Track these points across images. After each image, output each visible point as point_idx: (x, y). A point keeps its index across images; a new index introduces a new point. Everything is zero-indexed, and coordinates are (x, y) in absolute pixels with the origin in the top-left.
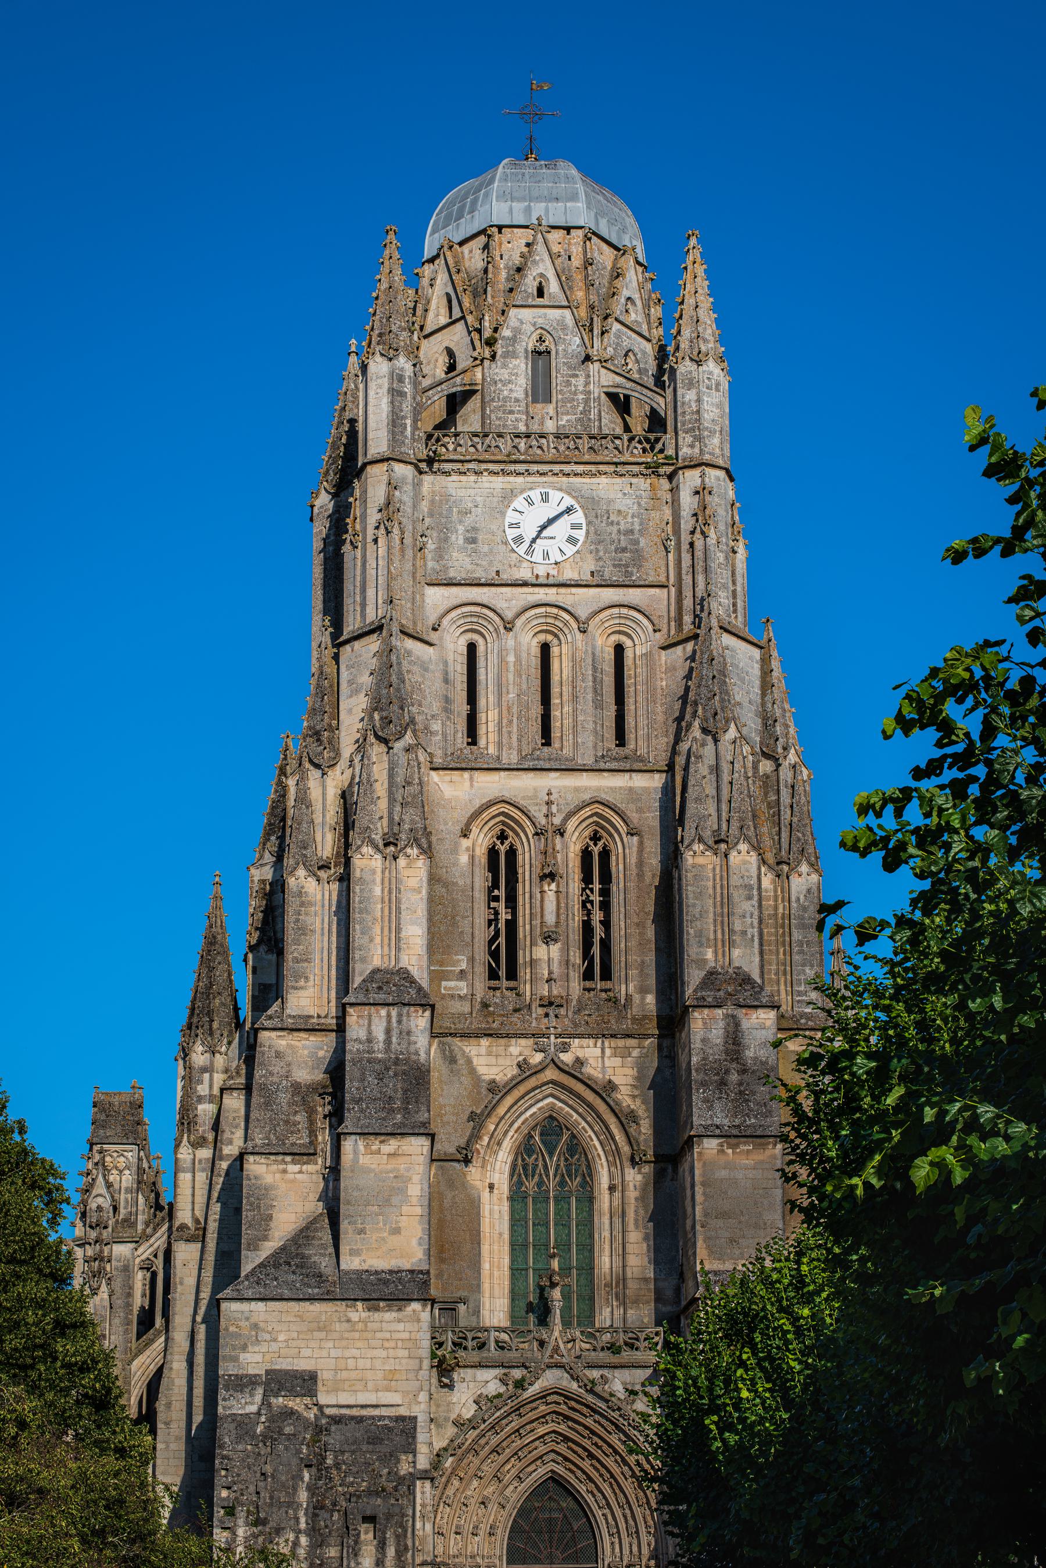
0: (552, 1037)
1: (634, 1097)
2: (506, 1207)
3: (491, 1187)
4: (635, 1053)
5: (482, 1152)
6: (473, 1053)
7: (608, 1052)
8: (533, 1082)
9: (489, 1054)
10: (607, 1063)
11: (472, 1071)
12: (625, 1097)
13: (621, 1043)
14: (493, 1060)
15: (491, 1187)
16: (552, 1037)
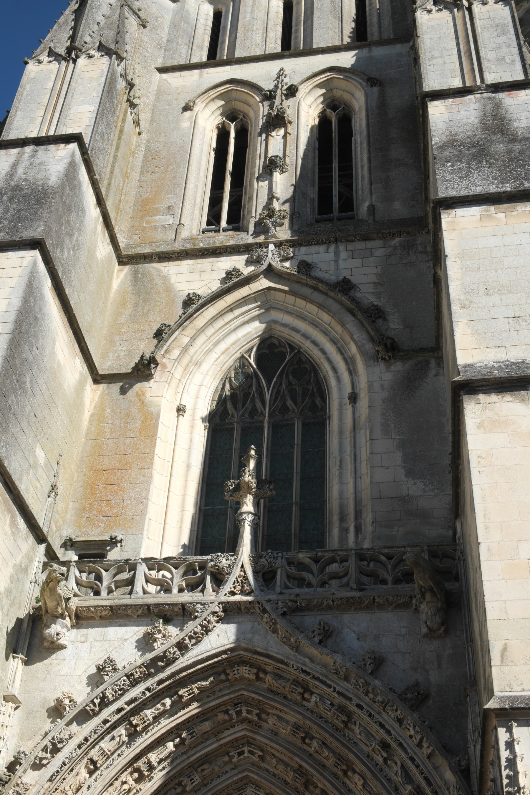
0: (271, 247)
1: (378, 295)
2: (200, 436)
3: (180, 410)
4: (379, 253)
5: (169, 366)
6: (171, 272)
7: (343, 255)
8: (245, 291)
9: (192, 272)
10: (342, 265)
11: (168, 288)
12: (367, 294)
13: (360, 245)
14: (196, 276)
15: (180, 410)
16: (271, 247)
